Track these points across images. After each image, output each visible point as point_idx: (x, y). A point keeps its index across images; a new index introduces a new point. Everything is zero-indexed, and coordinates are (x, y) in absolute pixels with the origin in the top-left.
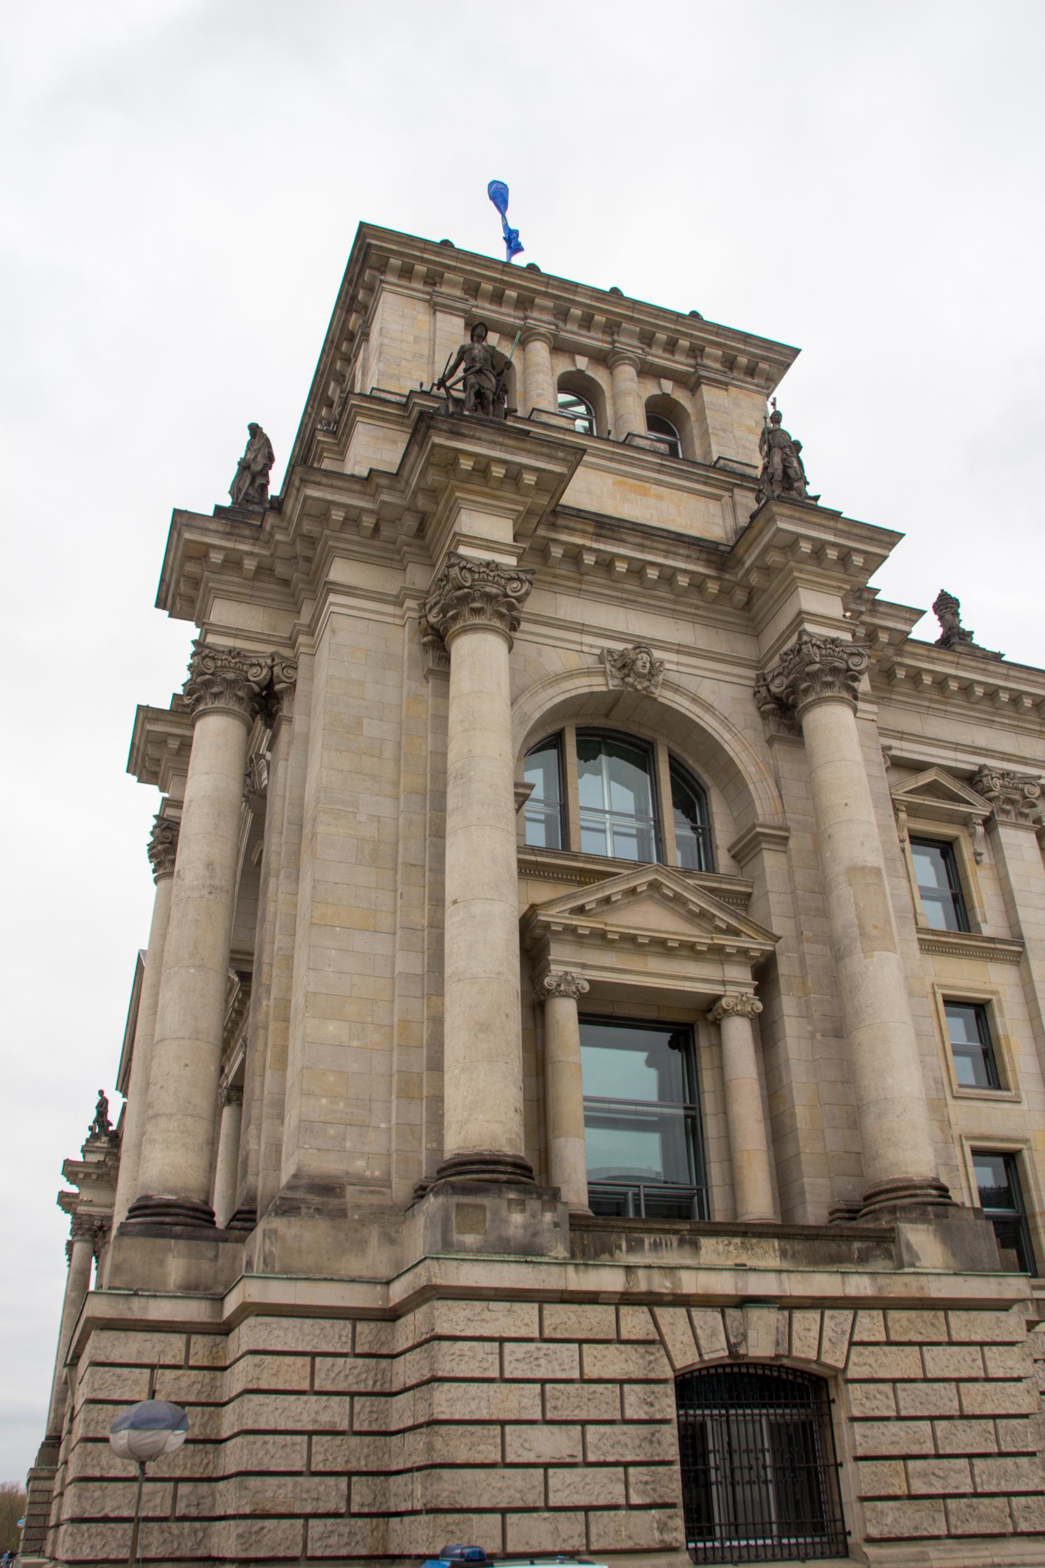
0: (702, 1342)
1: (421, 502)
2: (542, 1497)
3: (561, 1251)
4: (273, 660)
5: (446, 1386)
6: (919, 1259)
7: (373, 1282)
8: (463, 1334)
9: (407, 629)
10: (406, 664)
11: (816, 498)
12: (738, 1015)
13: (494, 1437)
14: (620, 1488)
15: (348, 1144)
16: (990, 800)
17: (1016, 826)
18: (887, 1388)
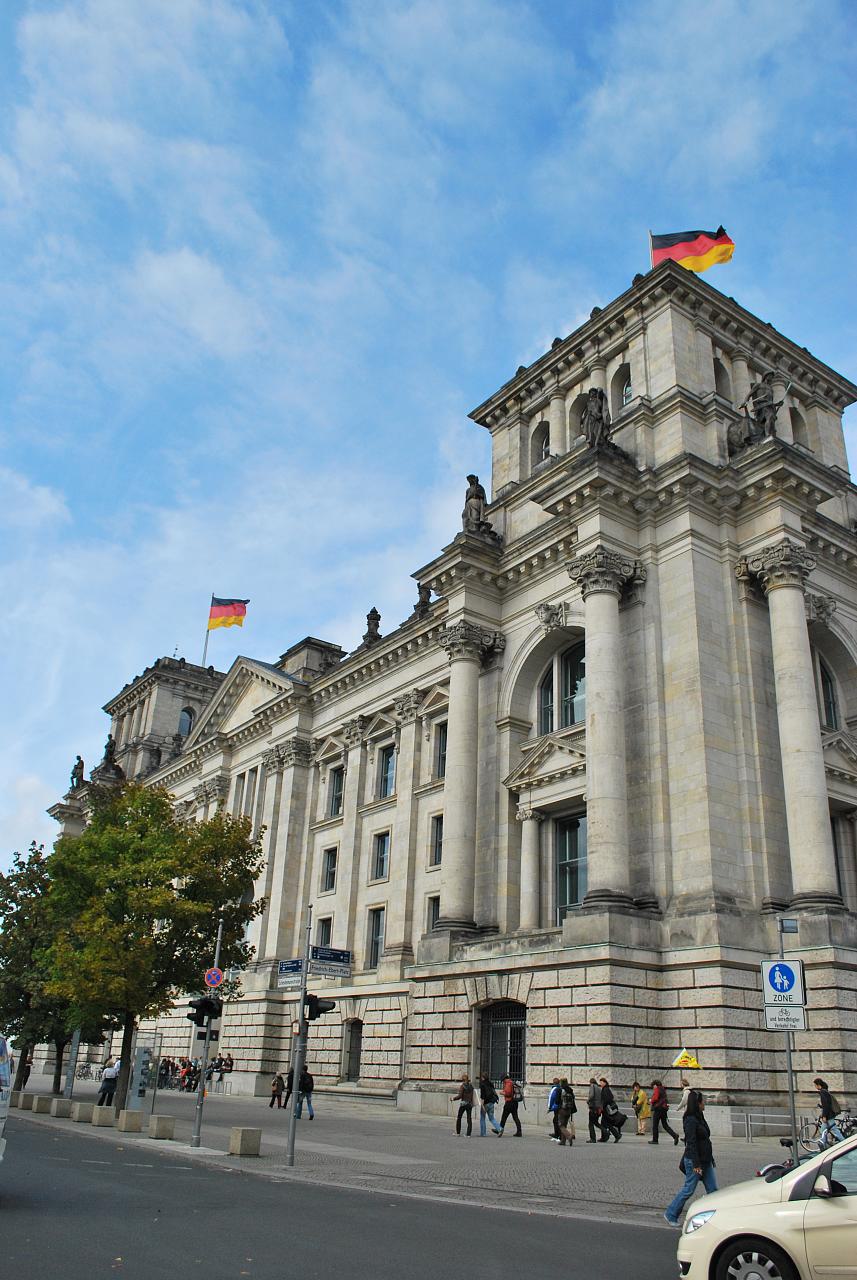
15: (730, 875)
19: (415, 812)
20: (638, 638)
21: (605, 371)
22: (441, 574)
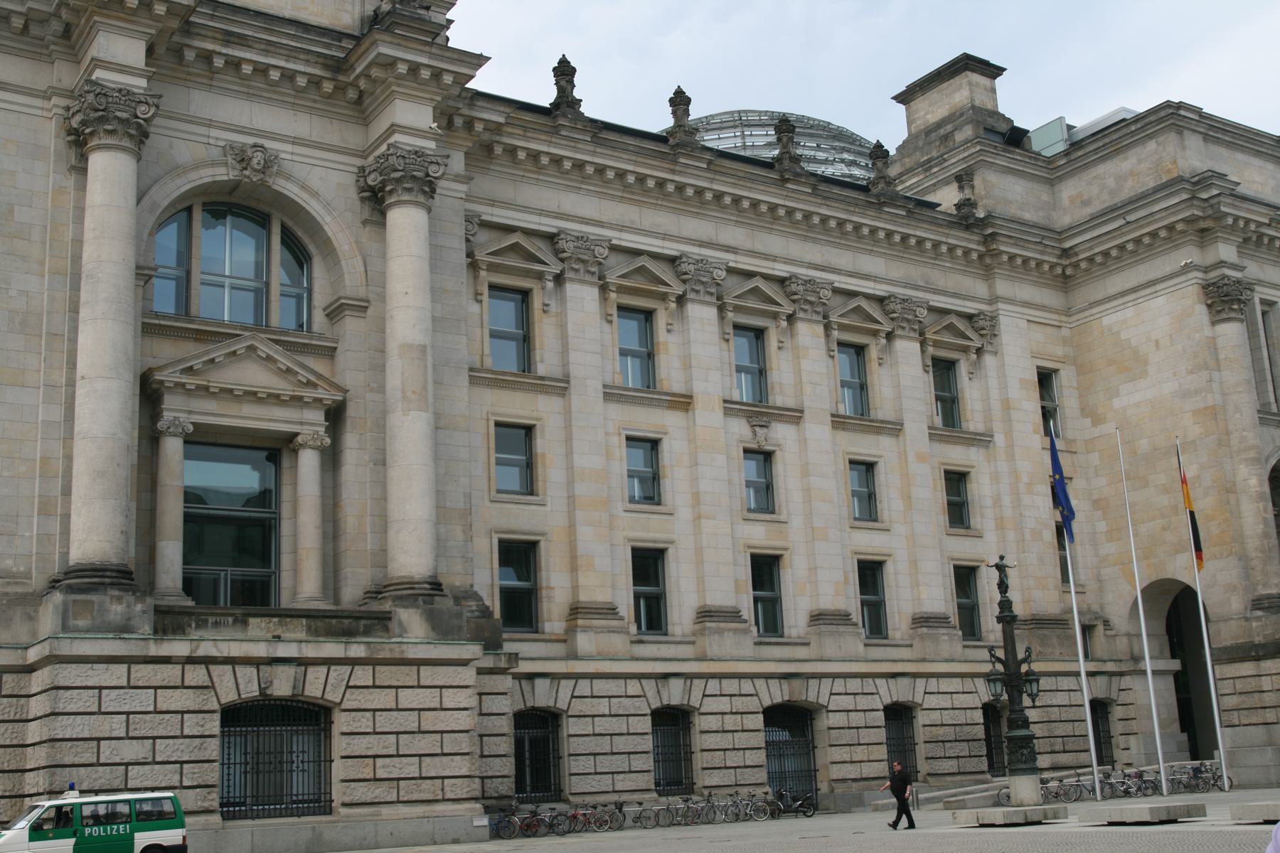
0: (241, 687)
1: (65, 14)
2: (124, 782)
3: (147, 629)
5: (60, 718)
6: (406, 631)
7: (16, 647)
8: (74, 685)
9: (54, 119)
10: (52, 159)
12: (310, 448)
13: (92, 748)
14: (177, 777)
16: (562, 260)
17: (582, 282)
18: (369, 714)
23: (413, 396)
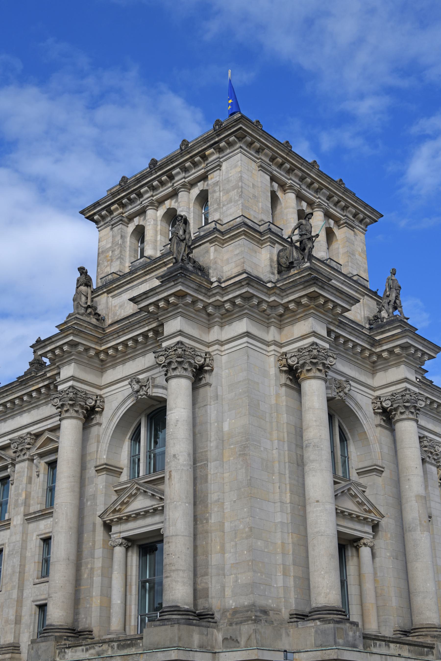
4: (206, 355)
11: (407, 319)
19: (25, 533)
20: (206, 411)
21: (189, 193)
22: (55, 348)
23: (425, 524)
